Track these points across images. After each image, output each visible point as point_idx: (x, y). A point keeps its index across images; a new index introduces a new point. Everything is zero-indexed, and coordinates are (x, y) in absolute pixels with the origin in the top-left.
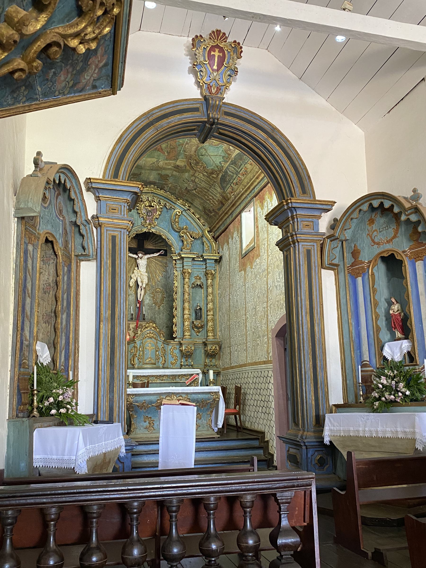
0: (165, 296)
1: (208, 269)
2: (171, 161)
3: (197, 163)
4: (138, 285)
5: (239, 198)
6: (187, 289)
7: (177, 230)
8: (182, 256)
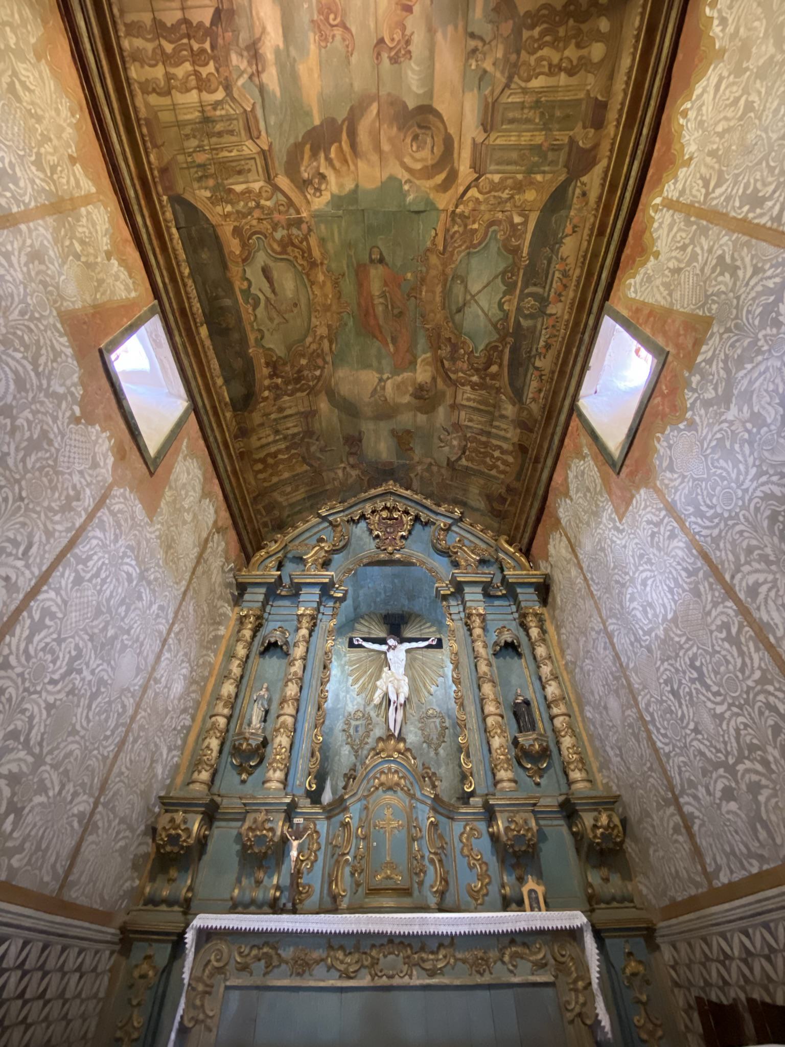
0: (447, 724)
1: (523, 604)
2: (406, 375)
3: (455, 348)
5: (562, 372)
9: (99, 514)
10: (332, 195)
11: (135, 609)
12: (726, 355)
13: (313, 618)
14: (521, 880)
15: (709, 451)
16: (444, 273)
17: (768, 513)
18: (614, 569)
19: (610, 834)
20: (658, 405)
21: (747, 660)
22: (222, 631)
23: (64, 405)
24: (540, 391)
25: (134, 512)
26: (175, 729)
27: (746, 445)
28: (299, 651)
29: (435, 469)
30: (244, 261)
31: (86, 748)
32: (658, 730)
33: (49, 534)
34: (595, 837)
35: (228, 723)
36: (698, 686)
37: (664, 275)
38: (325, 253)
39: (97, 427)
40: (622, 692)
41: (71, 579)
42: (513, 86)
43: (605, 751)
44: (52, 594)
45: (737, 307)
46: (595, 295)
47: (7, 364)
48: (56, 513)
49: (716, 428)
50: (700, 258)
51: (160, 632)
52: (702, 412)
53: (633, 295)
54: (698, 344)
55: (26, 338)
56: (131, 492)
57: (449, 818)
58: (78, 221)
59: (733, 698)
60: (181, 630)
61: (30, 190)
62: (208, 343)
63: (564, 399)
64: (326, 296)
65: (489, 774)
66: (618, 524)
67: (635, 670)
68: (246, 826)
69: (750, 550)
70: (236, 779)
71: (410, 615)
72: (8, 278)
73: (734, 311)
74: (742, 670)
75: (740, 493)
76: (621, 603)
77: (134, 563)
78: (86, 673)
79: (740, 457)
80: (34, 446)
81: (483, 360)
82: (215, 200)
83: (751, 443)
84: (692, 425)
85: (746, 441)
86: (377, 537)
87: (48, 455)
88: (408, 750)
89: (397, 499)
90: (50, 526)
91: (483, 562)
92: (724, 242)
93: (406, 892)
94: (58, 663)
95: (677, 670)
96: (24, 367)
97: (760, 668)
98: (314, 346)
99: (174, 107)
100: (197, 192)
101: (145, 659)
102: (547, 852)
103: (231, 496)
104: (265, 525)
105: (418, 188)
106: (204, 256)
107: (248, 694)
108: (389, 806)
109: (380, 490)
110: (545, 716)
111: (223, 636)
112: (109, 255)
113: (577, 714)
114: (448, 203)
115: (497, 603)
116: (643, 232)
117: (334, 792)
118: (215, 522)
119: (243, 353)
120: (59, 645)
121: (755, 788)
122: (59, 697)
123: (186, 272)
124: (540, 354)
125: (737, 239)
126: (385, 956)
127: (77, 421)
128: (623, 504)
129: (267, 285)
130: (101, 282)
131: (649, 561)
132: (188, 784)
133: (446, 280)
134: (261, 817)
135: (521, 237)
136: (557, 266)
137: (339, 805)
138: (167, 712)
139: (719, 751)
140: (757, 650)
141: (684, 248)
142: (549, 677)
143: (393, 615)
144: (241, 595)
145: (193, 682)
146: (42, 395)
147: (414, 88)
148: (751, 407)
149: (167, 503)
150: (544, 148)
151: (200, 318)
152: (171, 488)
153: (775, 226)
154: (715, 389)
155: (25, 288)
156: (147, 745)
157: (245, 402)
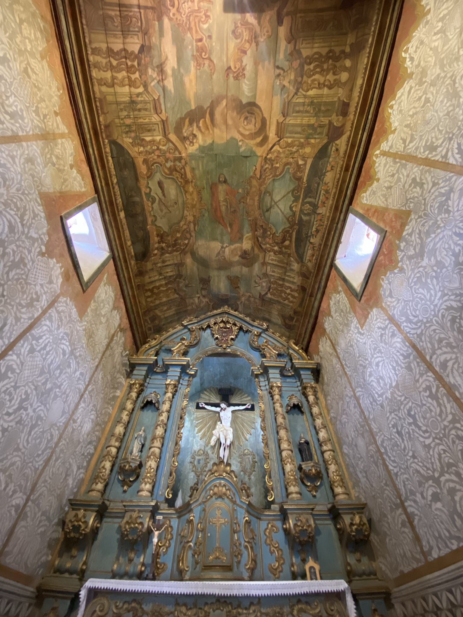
0: (256, 460)
1: (304, 381)
4: (221, 443)
5: (326, 245)
9: (50, 311)
10: (199, 145)
11: (66, 373)
12: (420, 231)
13: (175, 386)
14: (304, 561)
15: (413, 284)
16: (260, 190)
17: (450, 318)
18: (358, 357)
19: (361, 529)
20: (382, 260)
21: (443, 409)
22: (118, 393)
23: (36, 244)
24: (313, 255)
25: (71, 313)
26: (83, 454)
27: (435, 280)
28: (165, 407)
29: (252, 299)
30: (148, 177)
31: (25, 460)
32: (389, 457)
33: (17, 319)
34: (352, 531)
35: (118, 453)
36: (413, 427)
37: (382, 190)
38: (194, 177)
39: (54, 260)
40: (366, 435)
41: (28, 349)
42: (299, 94)
43: (356, 475)
44: (15, 357)
45: (424, 204)
46: (344, 202)
47: (5, 217)
48: (23, 307)
49: (416, 271)
50: (402, 180)
51: (80, 390)
52: (408, 262)
53: (365, 202)
54: (403, 225)
55: (18, 203)
56: (71, 300)
58: (56, 146)
59: (436, 433)
60: (93, 390)
61: (30, 124)
62: (124, 221)
63: (327, 259)
64: (193, 199)
65: (284, 490)
66: (360, 330)
67: (374, 419)
68: (125, 520)
69: (440, 341)
70: (120, 490)
71: (235, 389)
72: (12, 169)
73: (423, 207)
74: (440, 415)
75: (432, 307)
76: (364, 378)
77: (67, 344)
78: (30, 410)
79: (431, 286)
80: (15, 265)
81: (280, 238)
82: (134, 144)
83: (437, 278)
84: (402, 270)
85: (434, 277)
86: (217, 338)
87: (23, 272)
88: (232, 471)
89: (230, 317)
90: (18, 314)
91: (279, 355)
92: (416, 171)
93: (228, 568)
94: (13, 402)
95: (400, 417)
96: (15, 220)
97: (451, 413)
98: (185, 227)
99: (115, 94)
100: (125, 139)
101: (69, 406)
102: (321, 542)
103: (130, 310)
104: (150, 329)
105: (247, 144)
106: (126, 173)
107: (131, 434)
108: (219, 508)
109: (219, 311)
110: (319, 452)
111: (118, 397)
112: (72, 167)
113: (338, 451)
114: (263, 153)
115: (288, 380)
116: (371, 168)
117: (183, 500)
118: (120, 325)
119: (144, 228)
120: (15, 390)
121: (452, 492)
122: (10, 424)
123: (115, 181)
124: (313, 235)
125: (423, 169)
126: (214, 611)
127: (43, 255)
128: (363, 318)
129: (160, 191)
130: (65, 180)
131: (380, 351)
132: (89, 491)
133: (260, 194)
134: (135, 515)
135: (303, 171)
136: (322, 188)
137: (187, 508)
138: (79, 442)
139: (428, 469)
140: (449, 402)
141: (393, 175)
143: (225, 389)
144: (132, 371)
145: (97, 424)
146: (24, 237)
147: (246, 93)
148: (435, 258)
149: (92, 310)
150: (315, 126)
151: (120, 206)
152: (95, 301)
153: (444, 160)
154: (415, 249)
155: (21, 177)
156: (64, 463)
157: (143, 256)
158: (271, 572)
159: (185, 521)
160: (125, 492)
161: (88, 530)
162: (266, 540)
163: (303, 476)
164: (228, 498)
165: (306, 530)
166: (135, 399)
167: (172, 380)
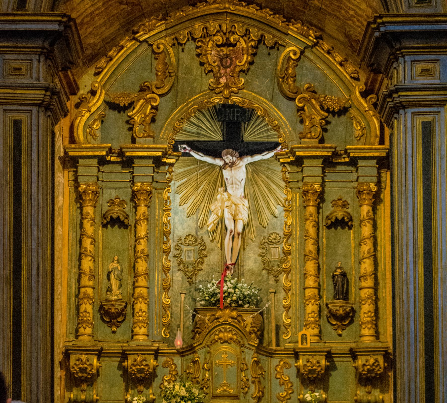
6: (312, 231)
7: (291, 95)
8: (297, 154)
13: (151, 192)
28: (142, 231)
57: (269, 356)
70: (108, 330)
86: (211, 71)
107: (101, 263)
115: (339, 168)
134: (139, 359)
142: (366, 255)
158: (279, 399)
159: (190, 361)
160: (114, 332)
161: (94, 371)
162: (276, 375)
163: (329, 314)
164: (234, 342)
165: (315, 369)
166: (93, 216)
167: (142, 184)
